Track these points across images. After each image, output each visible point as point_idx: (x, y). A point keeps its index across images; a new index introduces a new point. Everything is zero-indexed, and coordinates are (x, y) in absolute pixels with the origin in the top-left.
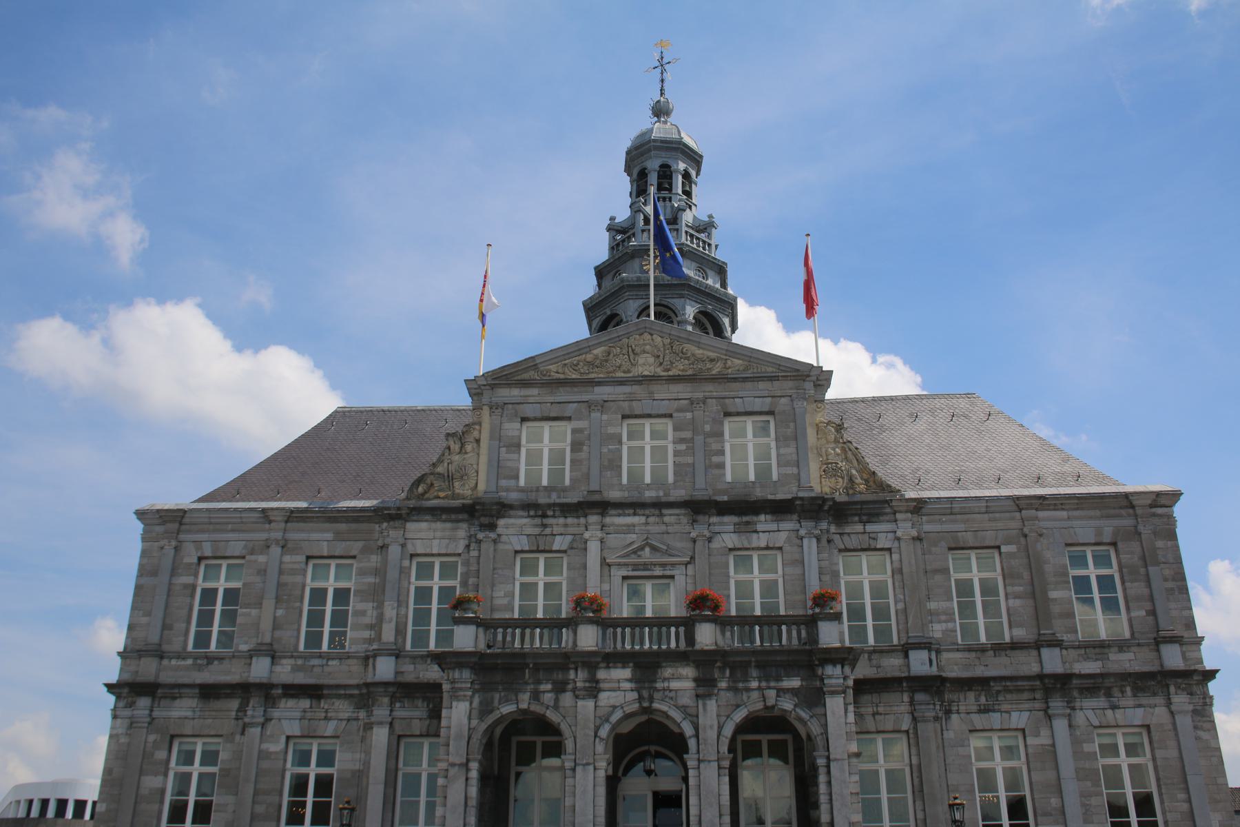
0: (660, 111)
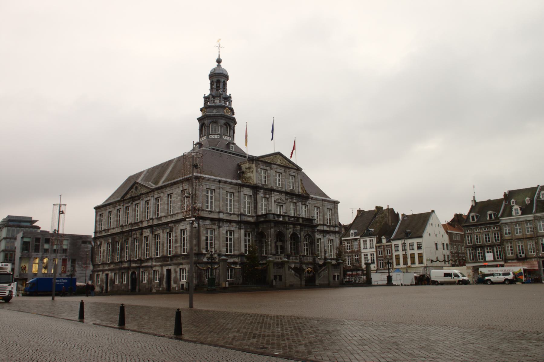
0: (219, 61)
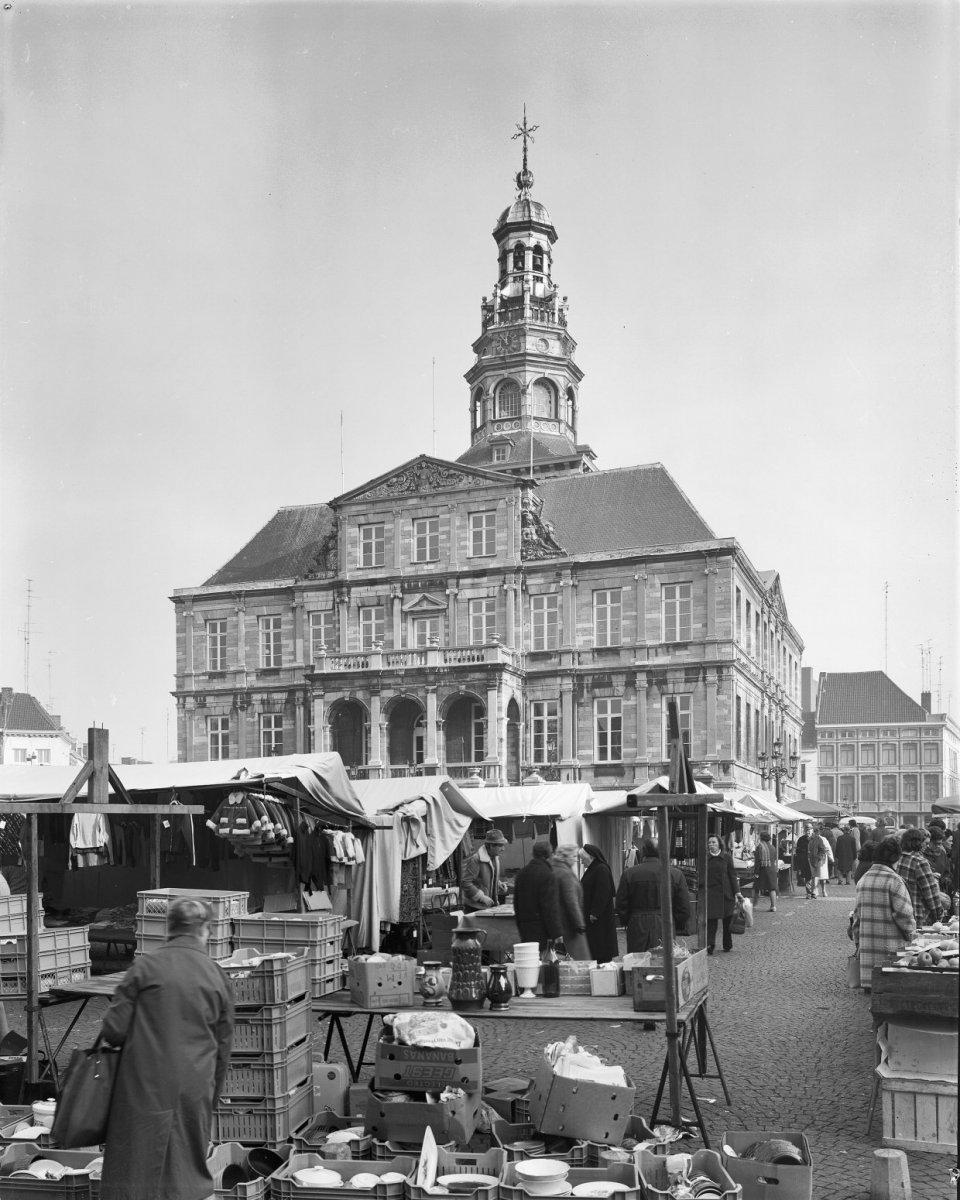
0: (523, 182)
